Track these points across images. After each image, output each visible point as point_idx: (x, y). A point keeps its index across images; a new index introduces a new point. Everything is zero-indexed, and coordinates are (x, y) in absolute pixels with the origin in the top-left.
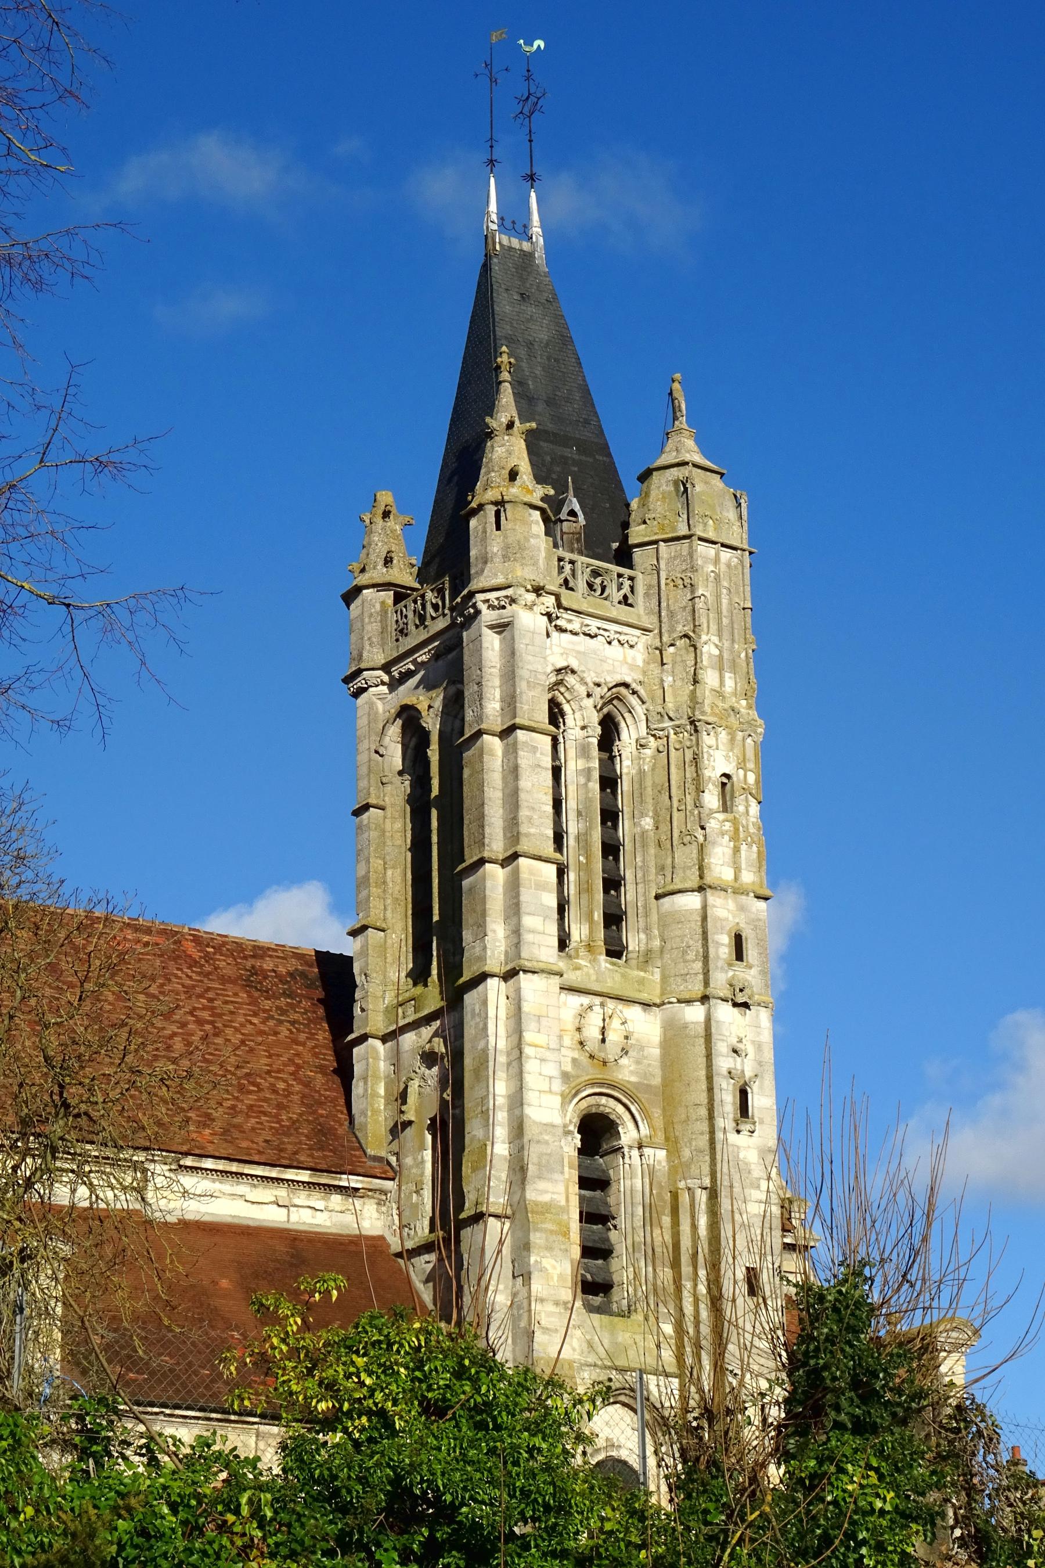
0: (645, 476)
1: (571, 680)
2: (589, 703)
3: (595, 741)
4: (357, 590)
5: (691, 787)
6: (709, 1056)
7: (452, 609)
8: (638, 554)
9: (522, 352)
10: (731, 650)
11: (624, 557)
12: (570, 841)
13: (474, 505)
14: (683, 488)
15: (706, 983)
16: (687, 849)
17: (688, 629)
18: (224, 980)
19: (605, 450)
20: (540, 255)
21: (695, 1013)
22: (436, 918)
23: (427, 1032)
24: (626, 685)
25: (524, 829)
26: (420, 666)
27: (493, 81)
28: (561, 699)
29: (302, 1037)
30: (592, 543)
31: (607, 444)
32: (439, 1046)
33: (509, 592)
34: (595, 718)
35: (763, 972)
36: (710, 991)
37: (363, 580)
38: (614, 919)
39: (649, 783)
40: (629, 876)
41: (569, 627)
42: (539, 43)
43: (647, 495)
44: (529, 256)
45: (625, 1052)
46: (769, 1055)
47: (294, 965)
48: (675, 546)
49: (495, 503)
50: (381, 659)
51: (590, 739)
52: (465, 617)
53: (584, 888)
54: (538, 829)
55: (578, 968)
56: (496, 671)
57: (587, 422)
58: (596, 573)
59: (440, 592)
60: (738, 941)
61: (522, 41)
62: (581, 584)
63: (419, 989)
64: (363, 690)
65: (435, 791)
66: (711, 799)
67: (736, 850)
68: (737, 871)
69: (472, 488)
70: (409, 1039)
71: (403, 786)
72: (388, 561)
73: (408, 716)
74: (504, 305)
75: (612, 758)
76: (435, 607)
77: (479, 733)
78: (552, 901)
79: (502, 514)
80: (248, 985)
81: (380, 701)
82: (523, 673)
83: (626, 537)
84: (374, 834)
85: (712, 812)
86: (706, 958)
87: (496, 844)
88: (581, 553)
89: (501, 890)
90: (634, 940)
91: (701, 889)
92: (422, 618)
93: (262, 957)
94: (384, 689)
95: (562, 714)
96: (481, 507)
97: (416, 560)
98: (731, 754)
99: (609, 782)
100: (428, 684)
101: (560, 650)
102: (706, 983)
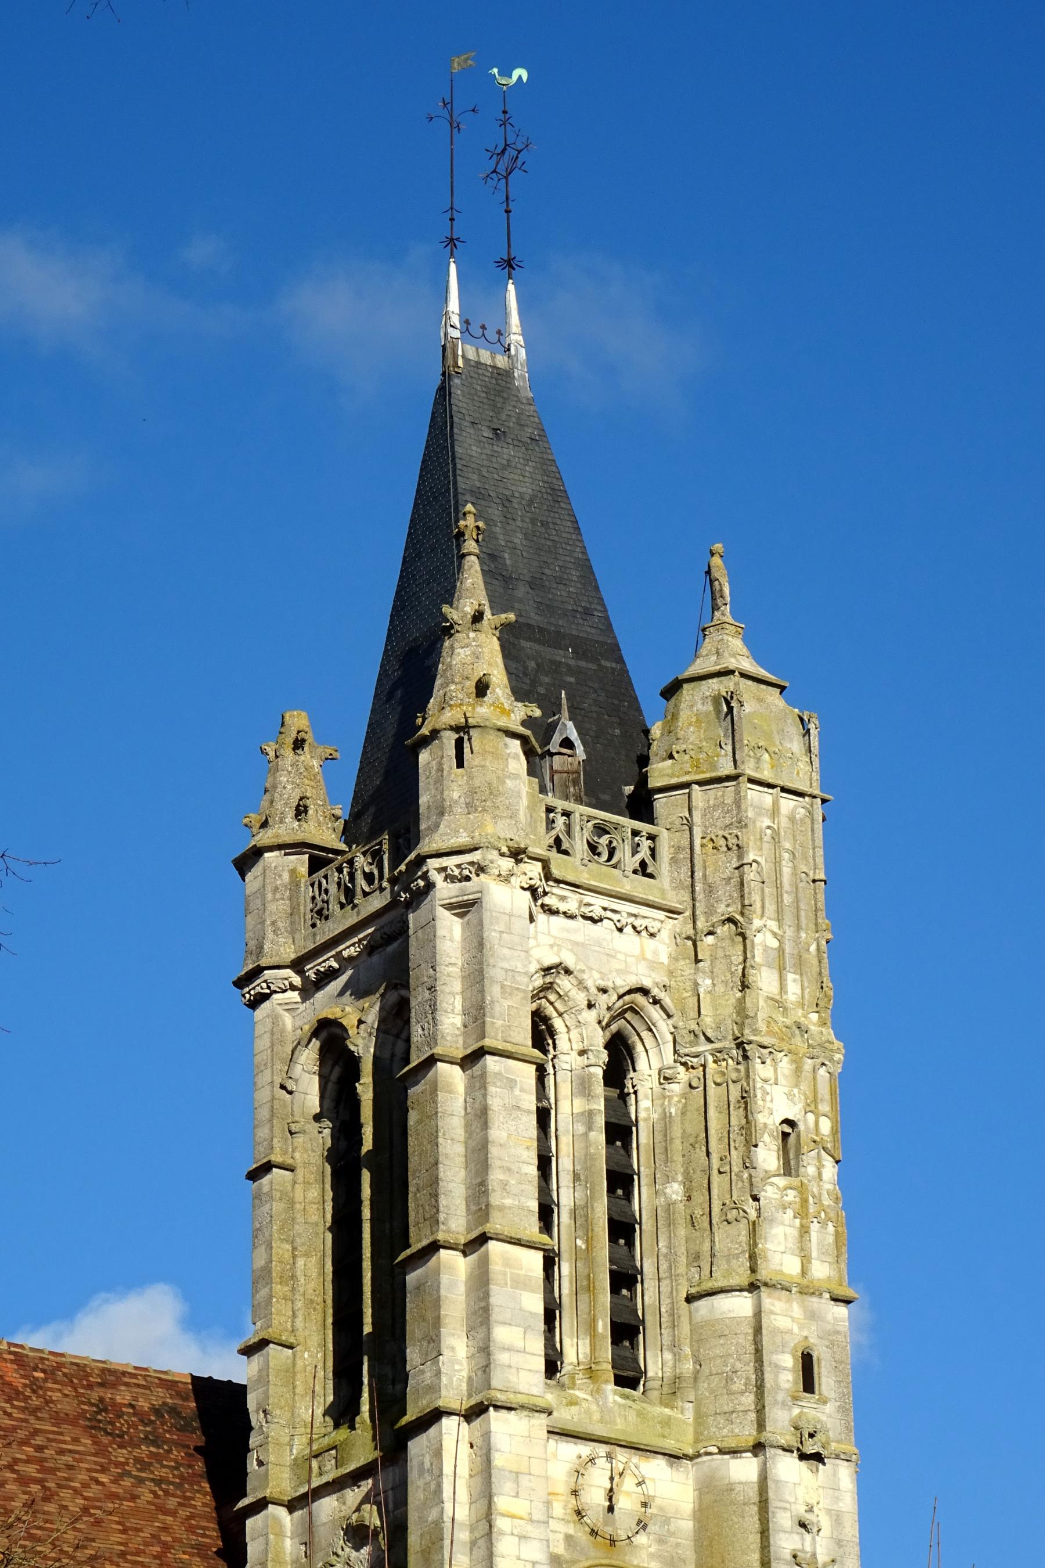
0: (671, 691)
1: (564, 983)
2: (590, 1016)
3: (599, 1072)
4: (257, 853)
5: (738, 1139)
6: (764, 1533)
7: (393, 881)
8: (661, 803)
9: (495, 512)
10: (797, 940)
11: (641, 806)
12: (563, 1218)
13: (425, 731)
14: (727, 708)
15: (761, 1425)
16: (733, 1229)
17: (733, 910)
18: (58, 1419)
19: (614, 651)
20: (521, 375)
21: (744, 1470)
22: (367, 1329)
23: (353, 1495)
24: (644, 991)
25: (495, 1199)
26: (346, 962)
27: (454, 126)
28: (550, 1011)
29: (172, 1503)
30: (595, 788)
31: (617, 645)
32: (372, 1518)
34: (599, 1039)
35: (842, 1409)
36: (767, 1436)
37: (264, 838)
38: (626, 1331)
39: (676, 1132)
40: (649, 1268)
41: (563, 907)
42: (520, 73)
43: (675, 717)
44: (504, 376)
45: (642, 1525)
46: (851, 1530)
47: (161, 1396)
48: (715, 792)
49: (457, 729)
50: (290, 953)
51: (592, 1069)
52: (410, 890)
53: (584, 1286)
54: (516, 1200)
55: (573, 1402)
56: (455, 971)
57: (588, 612)
58: (601, 830)
59: (376, 856)
60: (807, 1363)
61: (495, 70)
62: (579, 845)
63: (343, 1433)
64: (262, 998)
65: (368, 1145)
66: (768, 1156)
67: (804, 1231)
68: (806, 1260)
69: (423, 708)
70: (328, 1507)
71: (322, 1136)
72: (301, 811)
73: (330, 1036)
74: (470, 445)
75: (623, 1097)
76: (369, 878)
77: (431, 1061)
78: (536, 1305)
79: (466, 744)
80: (94, 1427)
81: (288, 1014)
82: (496, 973)
83: (644, 779)
84: (278, 1207)
85: (768, 1175)
86: (760, 1388)
87: (455, 1222)
88: (579, 800)
89: (462, 1288)
90: (655, 1362)
91: (753, 1287)
92: (350, 894)
93: (114, 1386)
94: (295, 996)
95: (552, 1032)
96: (435, 733)
97: (342, 810)
98: (796, 1091)
99: (619, 1132)
100: (358, 990)
101: (550, 940)
102: (761, 1425)
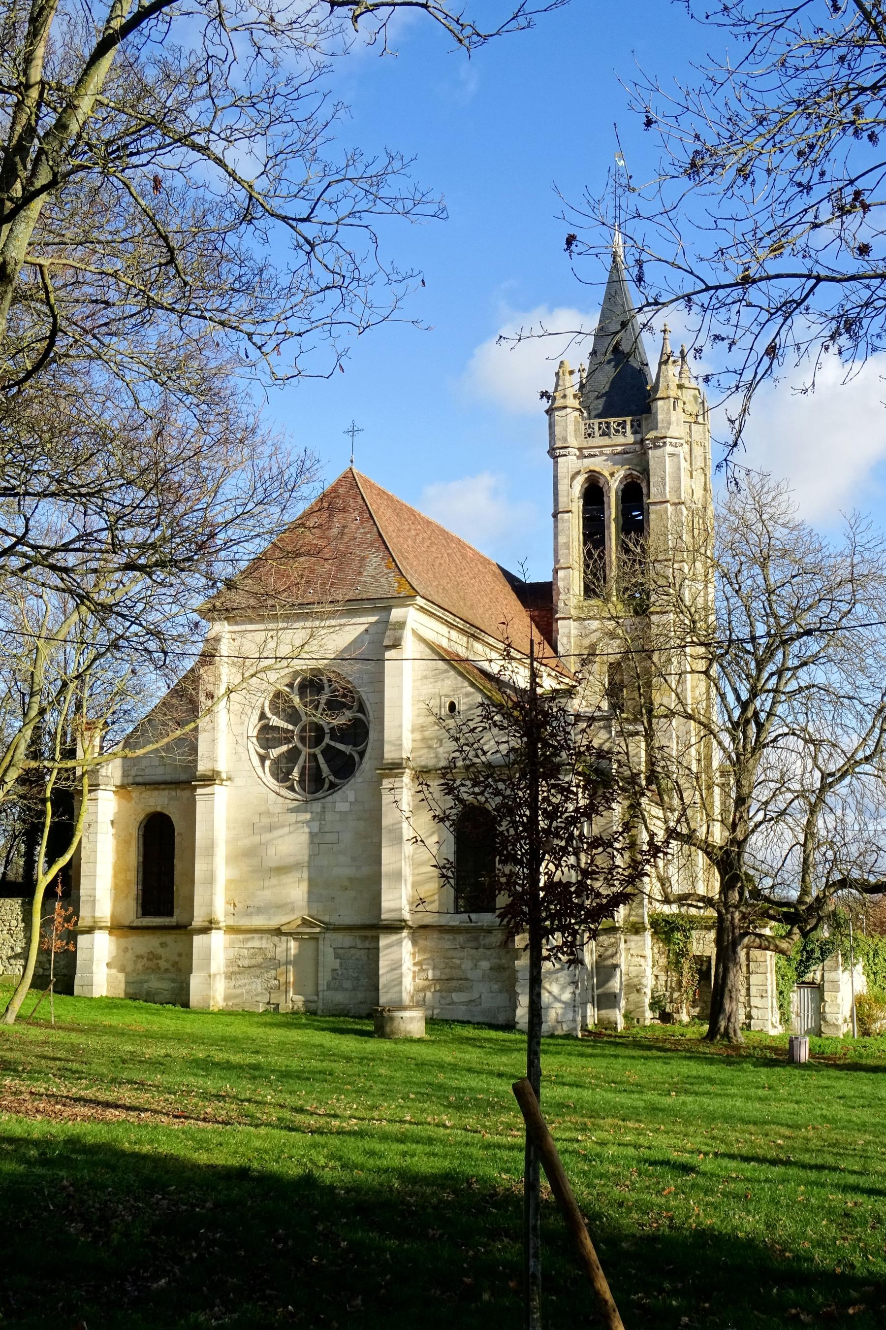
17: (703, 465)
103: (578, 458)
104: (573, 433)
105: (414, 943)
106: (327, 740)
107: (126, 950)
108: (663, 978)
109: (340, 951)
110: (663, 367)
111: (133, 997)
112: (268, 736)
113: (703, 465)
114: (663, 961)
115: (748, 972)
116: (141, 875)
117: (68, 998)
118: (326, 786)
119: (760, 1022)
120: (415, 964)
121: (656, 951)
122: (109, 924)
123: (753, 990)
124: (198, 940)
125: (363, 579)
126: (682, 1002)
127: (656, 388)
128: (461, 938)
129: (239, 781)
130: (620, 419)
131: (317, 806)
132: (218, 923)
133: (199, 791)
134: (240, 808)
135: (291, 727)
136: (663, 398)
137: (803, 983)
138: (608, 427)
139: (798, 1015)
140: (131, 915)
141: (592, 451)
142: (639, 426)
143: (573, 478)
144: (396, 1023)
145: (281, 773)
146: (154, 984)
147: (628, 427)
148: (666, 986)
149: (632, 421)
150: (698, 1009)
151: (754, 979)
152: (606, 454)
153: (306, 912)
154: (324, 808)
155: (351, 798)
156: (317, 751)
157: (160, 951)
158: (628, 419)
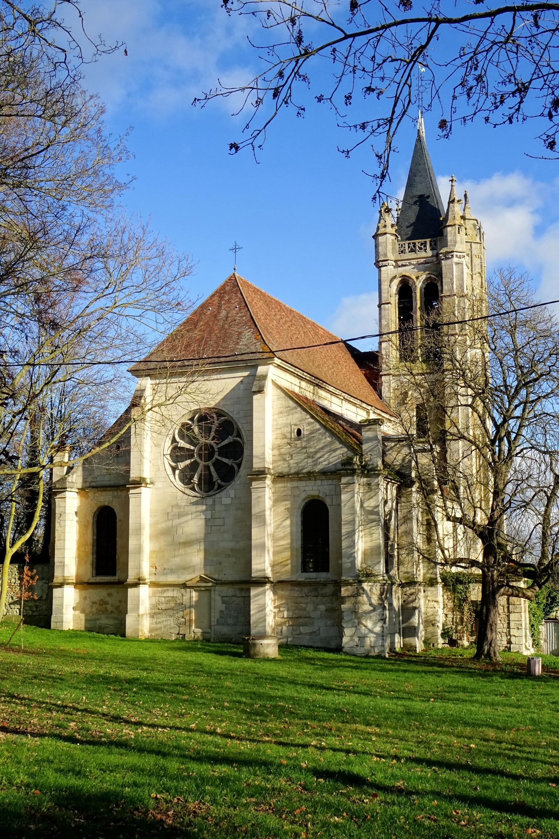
17: (480, 271)
33: (464, 254)
76: (421, 249)
103: (395, 267)
104: (391, 251)
105: (275, 593)
106: (216, 456)
107: (85, 598)
108: (450, 616)
109: (225, 598)
110: (451, 205)
111: (89, 629)
112: (177, 454)
113: (480, 271)
114: (450, 604)
115: (509, 612)
116: (95, 548)
117: (46, 631)
118: (216, 487)
119: (517, 646)
120: (275, 607)
121: (446, 597)
122: (74, 581)
123: (512, 625)
124: (131, 591)
125: (239, 347)
126: (463, 632)
127: (446, 219)
128: (306, 590)
129: (158, 485)
130: (422, 241)
131: (210, 501)
132: (145, 580)
133: (131, 491)
134: (158, 500)
135: (192, 448)
136: (451, 226)
137: (549, 619)
138: (414, 246)
139: (546, 641)
140: (88, 576)
141: (404, 263)
142: (435, 245)
143: (391, 281)
144: (257, 648)
145: (186, 479)
146: (104, 621)
147: (428, 246)
148: (453, 621)
149: (430, 242)
150: (474, 637)
151: (512, 617)
152: (413, 264)
153: (203, 572)
154: (214, 502)
155: (232, 495)
156: (210, 463)
157: (108, 599)
158: (428, 241)
